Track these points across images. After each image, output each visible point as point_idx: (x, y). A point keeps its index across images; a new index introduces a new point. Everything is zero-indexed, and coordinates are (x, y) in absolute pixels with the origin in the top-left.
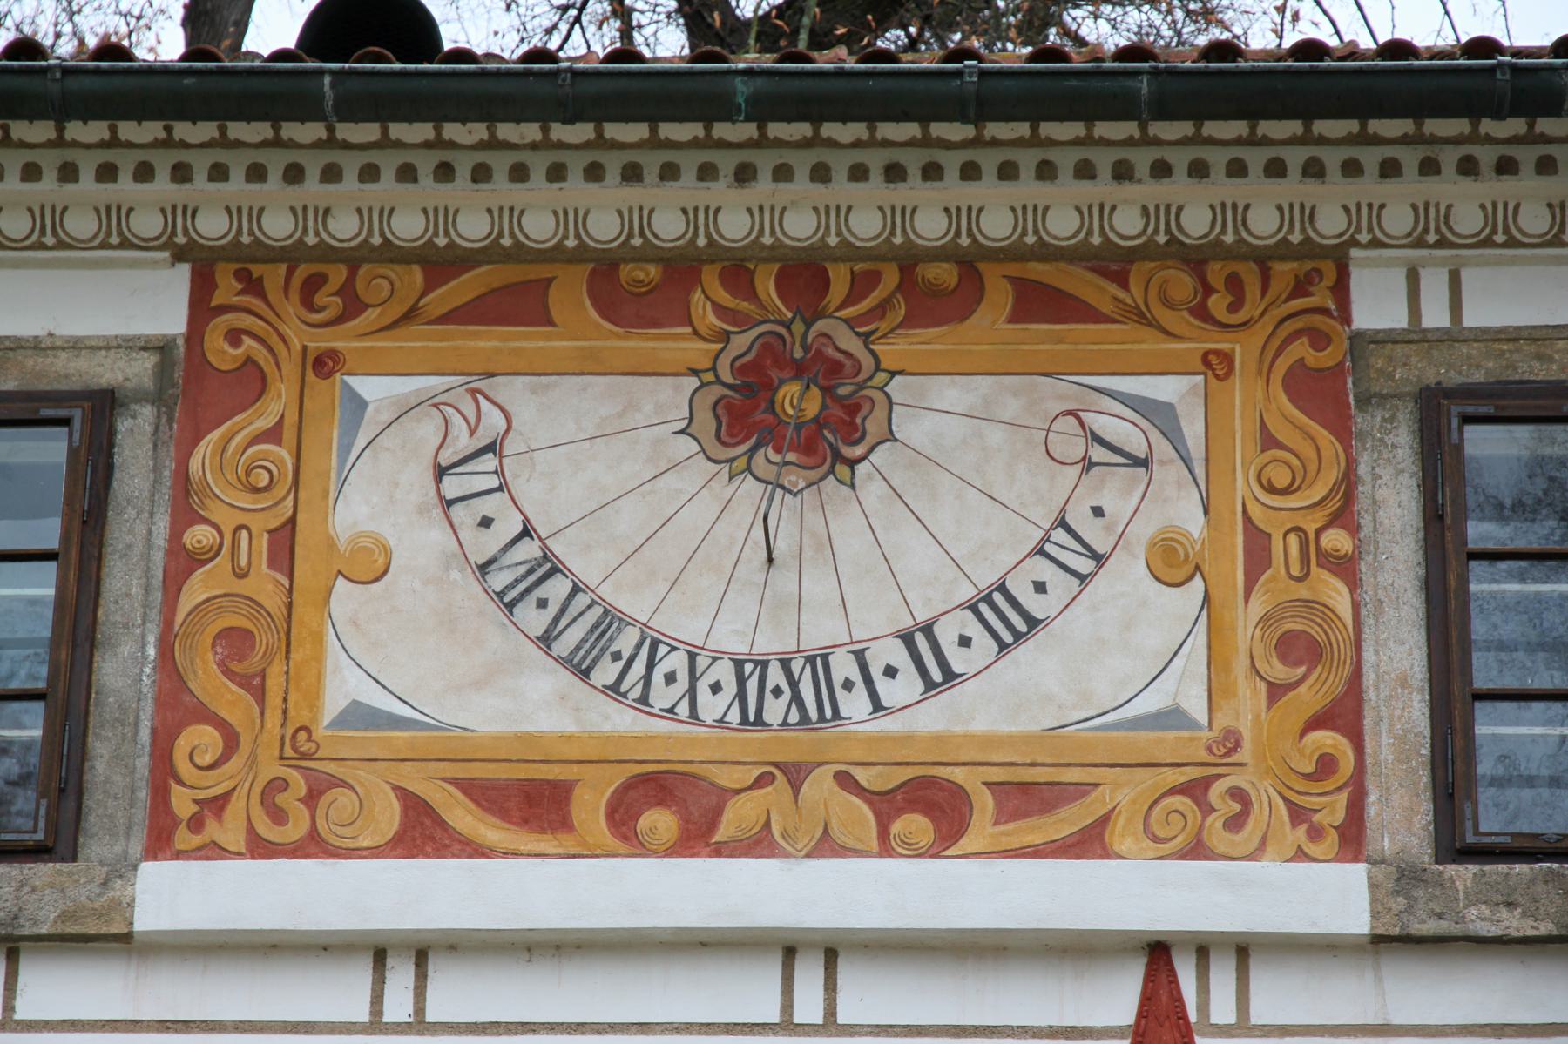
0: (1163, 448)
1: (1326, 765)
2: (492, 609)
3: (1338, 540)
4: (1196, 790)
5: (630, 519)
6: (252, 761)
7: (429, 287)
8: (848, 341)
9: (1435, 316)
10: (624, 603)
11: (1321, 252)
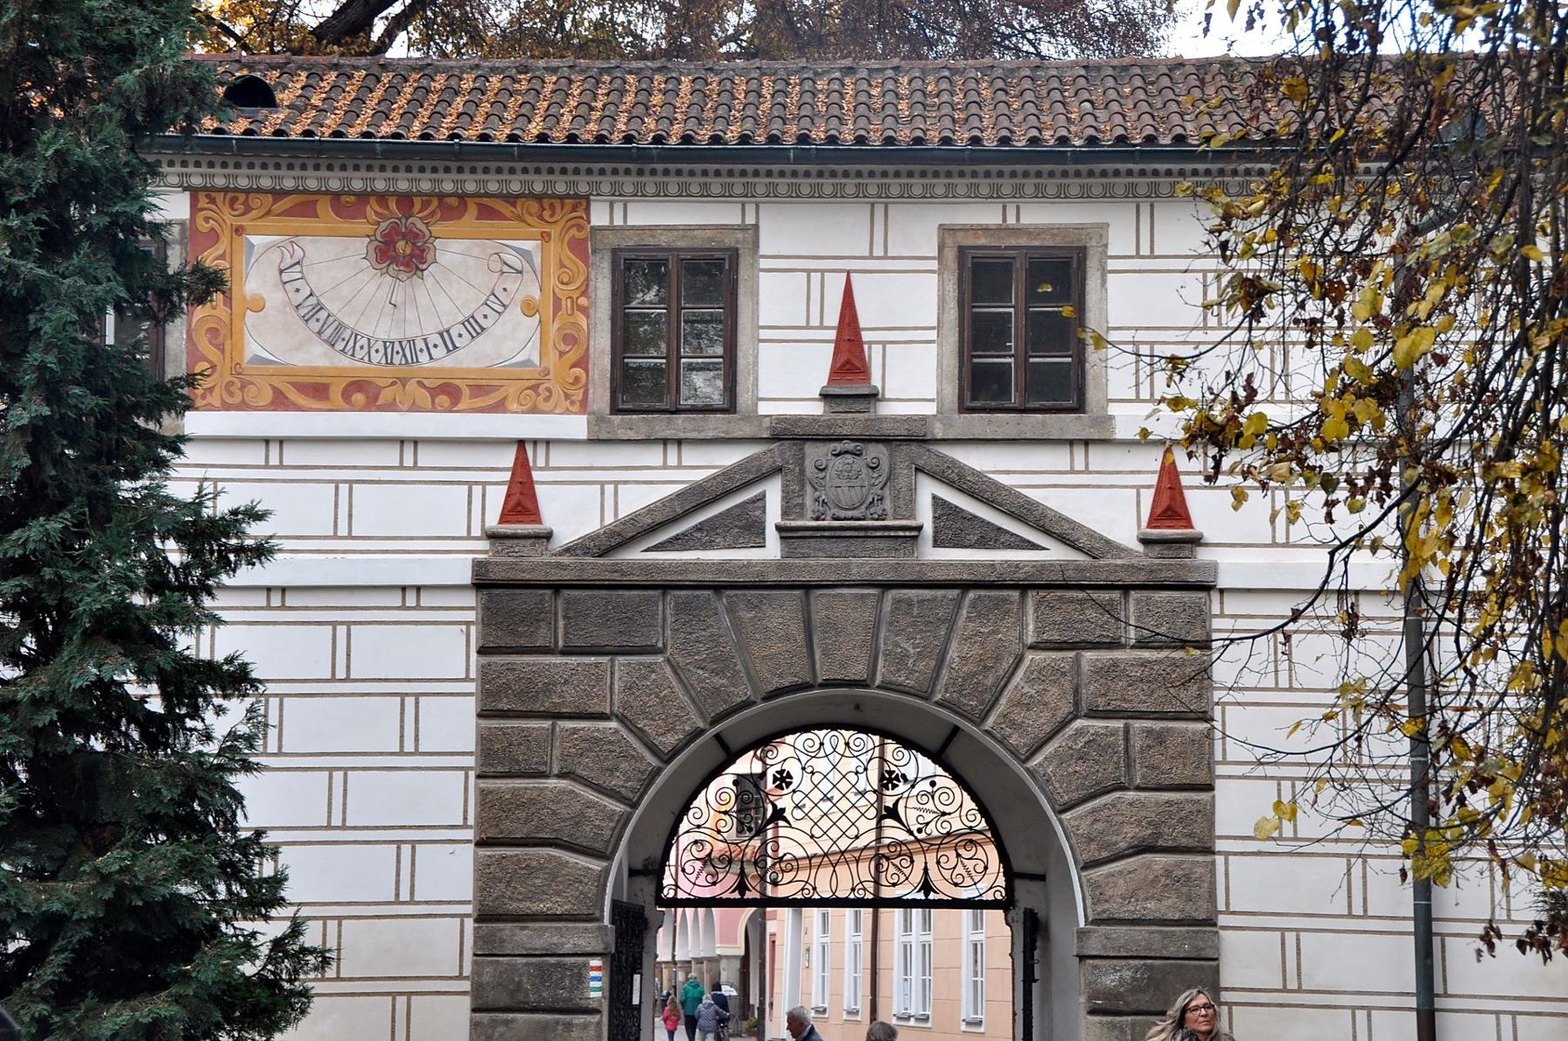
0: (527, 267)
1: (577, 380)
2: (301, 322)
3: (583, 301)
4: (535, 388)
5: (346, 290)
6: (221, 375)
7: (275, 201)
8: (422, 227)
9: (618, 221)
10: (345, 321)
11: (582, 197)
